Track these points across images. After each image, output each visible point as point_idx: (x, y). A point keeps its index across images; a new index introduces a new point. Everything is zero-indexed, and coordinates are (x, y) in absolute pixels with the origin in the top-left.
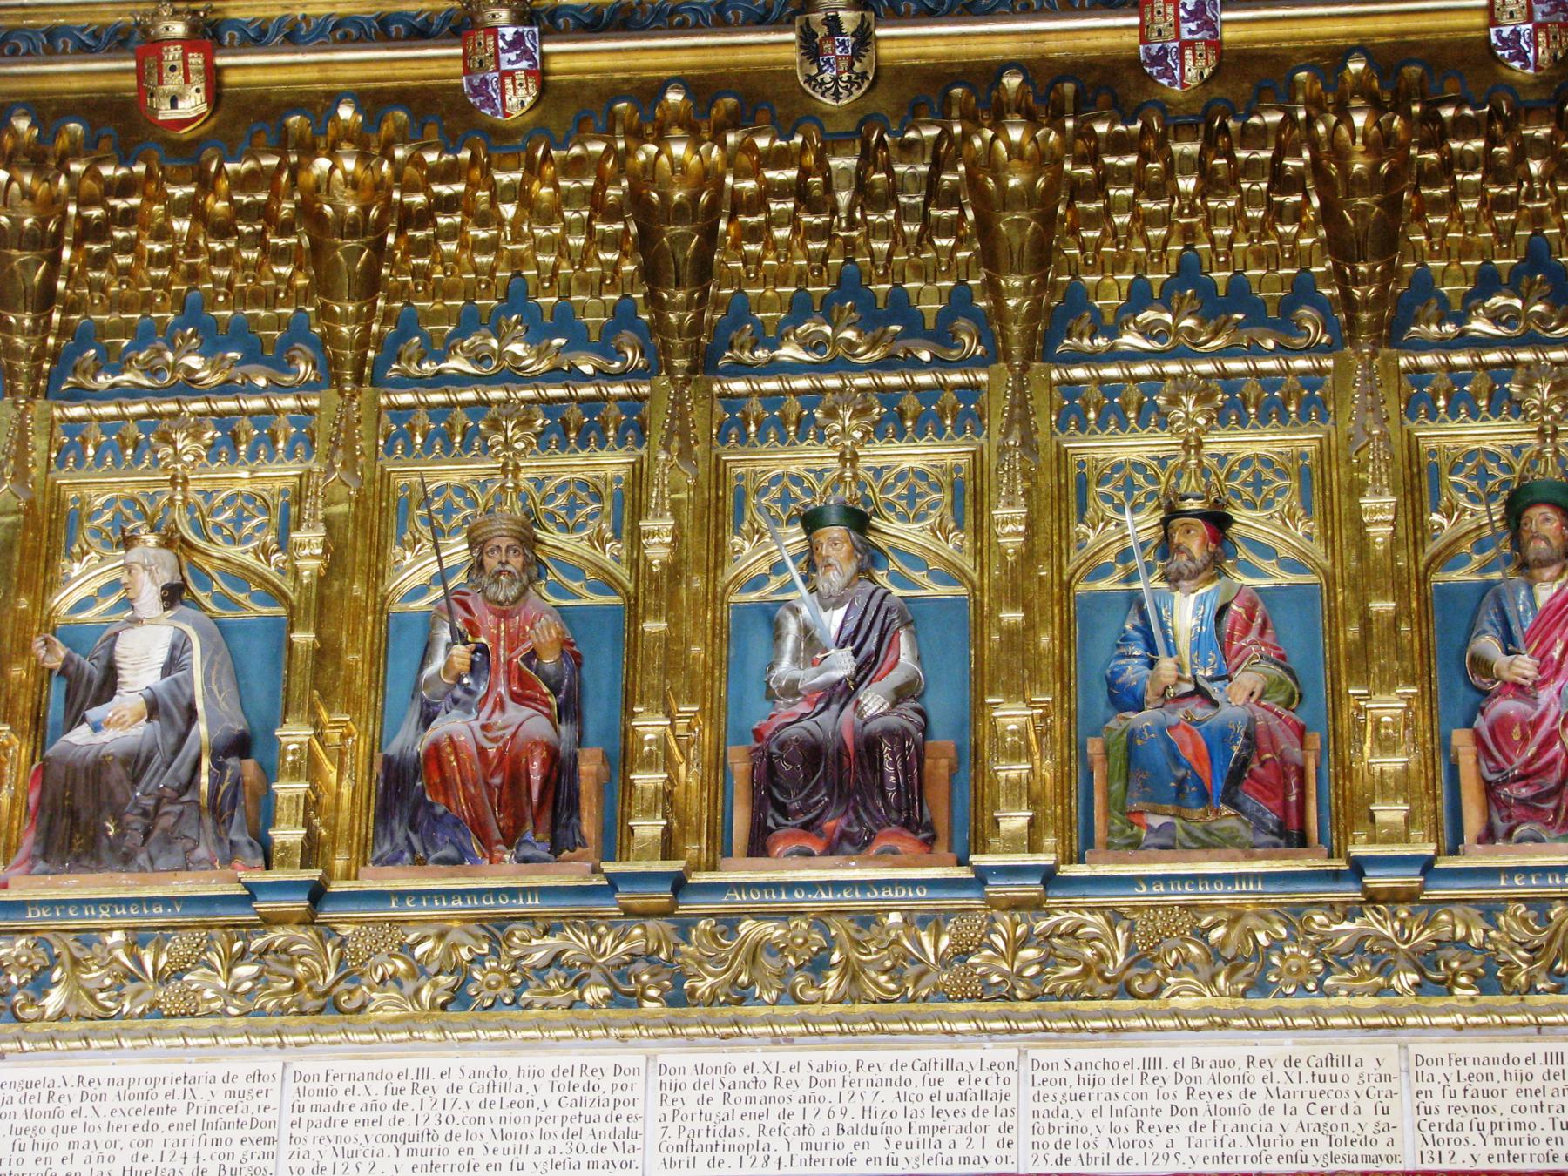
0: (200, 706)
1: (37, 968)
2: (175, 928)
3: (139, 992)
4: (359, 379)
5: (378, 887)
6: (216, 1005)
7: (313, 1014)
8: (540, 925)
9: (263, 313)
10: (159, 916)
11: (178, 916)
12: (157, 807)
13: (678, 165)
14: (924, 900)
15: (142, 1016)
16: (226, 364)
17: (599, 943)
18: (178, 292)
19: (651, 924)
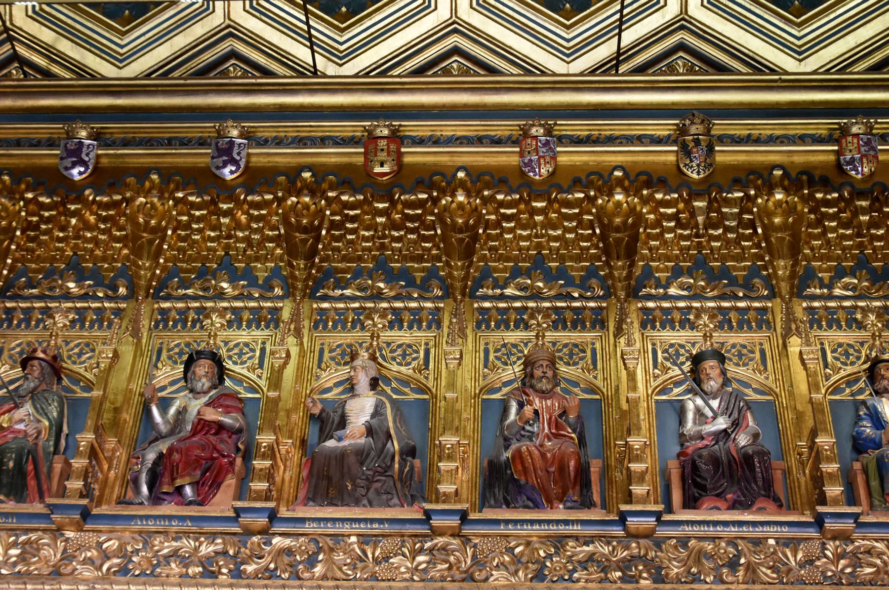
0: (392, 432)
1: (310, 553)
2: (383, 536)
3: (366, 567)
4: (463, 295)
5: (494, 517)
6: (407, 576)
7: (459, 581)
8: (582, 540)
9: (416, 266)
10: (376, 529)
11: (386, 528)
12: (373, 476)
13: (618, 204)
14: (786, 532)
15: (366, 580)
16: (398, 287)
17: (613, 550)
18: (375, 255)
19: (641, 541)
